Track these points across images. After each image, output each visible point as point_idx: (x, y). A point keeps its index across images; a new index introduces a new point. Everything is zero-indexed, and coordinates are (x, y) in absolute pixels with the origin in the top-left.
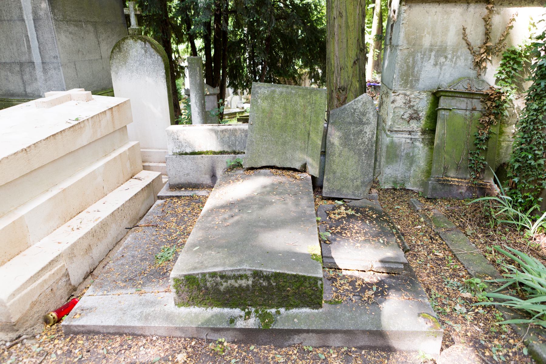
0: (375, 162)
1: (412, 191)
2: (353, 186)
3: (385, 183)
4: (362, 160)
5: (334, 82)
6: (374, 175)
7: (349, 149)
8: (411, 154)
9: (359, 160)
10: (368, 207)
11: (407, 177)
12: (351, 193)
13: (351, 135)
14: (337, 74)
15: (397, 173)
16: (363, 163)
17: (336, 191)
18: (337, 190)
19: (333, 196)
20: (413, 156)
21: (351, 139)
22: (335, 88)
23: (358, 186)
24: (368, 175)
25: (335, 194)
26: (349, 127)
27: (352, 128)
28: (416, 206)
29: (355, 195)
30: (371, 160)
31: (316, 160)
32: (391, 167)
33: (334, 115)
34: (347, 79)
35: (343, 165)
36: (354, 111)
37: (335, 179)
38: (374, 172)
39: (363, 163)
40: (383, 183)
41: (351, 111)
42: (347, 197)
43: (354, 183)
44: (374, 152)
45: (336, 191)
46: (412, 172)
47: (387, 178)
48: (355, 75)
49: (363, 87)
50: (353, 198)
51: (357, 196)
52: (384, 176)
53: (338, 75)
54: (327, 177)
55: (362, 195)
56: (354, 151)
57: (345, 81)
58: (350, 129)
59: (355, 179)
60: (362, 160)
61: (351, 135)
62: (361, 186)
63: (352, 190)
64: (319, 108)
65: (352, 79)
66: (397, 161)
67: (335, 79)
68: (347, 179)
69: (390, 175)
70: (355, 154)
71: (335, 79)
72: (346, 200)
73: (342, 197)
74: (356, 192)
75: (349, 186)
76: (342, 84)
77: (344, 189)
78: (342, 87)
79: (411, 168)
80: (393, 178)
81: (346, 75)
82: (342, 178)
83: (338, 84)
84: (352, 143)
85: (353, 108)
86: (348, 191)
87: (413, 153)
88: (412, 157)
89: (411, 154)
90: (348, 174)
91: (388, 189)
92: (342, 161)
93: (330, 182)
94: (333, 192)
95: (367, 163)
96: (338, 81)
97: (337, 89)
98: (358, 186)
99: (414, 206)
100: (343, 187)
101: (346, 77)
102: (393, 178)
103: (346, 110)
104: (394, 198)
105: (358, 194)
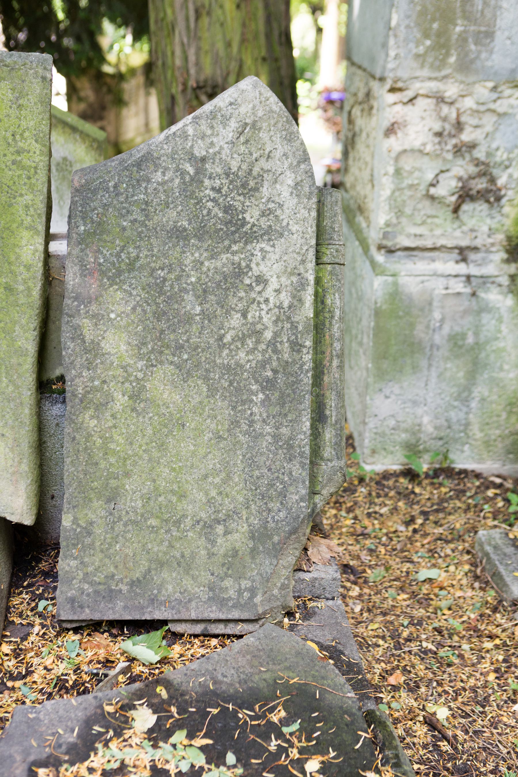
0: (314, 427)
1: (478, 476)
2: (211, 555)
3: (374, 452)
4: (251, 423)
5: (178, 62)
6: (313, 493)
7: (179, 367)
8: (470, 340)
9: (236, 423)
10: (287, 688)
11: (456, 427)
12: (203, 594)
13: (189, 297)
14: (184, 33)
15: (419, 411)
16: (257, 437)
17: (125, 588)
18: (132, 584)
19: (111, 616)
20: (478, 346)
21: (189, 319)
22: (180, 88)
23: (235, 553)
24: (283, 494)
25: (120, 604)
26: (176, 253)
27: (188, 260)
28: (508, 579)
29: (222, 603)
30: (297, 421)
32: (396, 389)
33: (95, 192)
34: (222, 53)
35: (155, 454)
36: (197, 173)
37: (119, 527)
38: (313, 477)
39: (257, 437)
40: (367, 451)
41: (183, 173)
42: (184, 616)
43: (213, 542)
44: (307, 379)
45: (125, 588)
46: (474, 404)
47: (383, 435)
48: (250, 36)
49: (286, 82)
50: (213, 616)
51: (234, 606)
52: (371, 425)
53: (189, 38)
54: (75, 521)
55: (258, 599)
56: (206, 379)
57: (216, 60)
58: (181, 264)
59: (218, 522)
60: (251, 423)
61: (189, 297)
62: (254, 552)
63: (205, 577)
64: (10, 157)
65: (240, 51)
66: (415, 368)
67: (178, 52)
68: (178, 523)
69: (392, 423)
70: (212, 391)
71: (178, 52)
72: (179, 628)
73: (158, 616)
74: (228, 583)
75: (193, 556)
76: (208, 70)
77: (165, 574)
78: (206, 81)
79: (470, 392)
80: (406, 431)
81: (219, 37)
82: (153, 522)
83: (192, 71)
84: (194, 340)
85: (192, 158)
86: (188, 583)
87: (476, 334)
88: (472, 349)
89: (470, 340)
90: (182, 496)
91: (386, 476)
92: (149, 431)
93: (92, 546)
95: (276, 437)
96: (192, 58)
97: (189, 91)
98: (235, 553)
99: (496, 575)
100: (161, 564)
101: (220, 46)
102: (406, 431)
103: (157, 166)
104: (412, 520)
105: (240, 592)
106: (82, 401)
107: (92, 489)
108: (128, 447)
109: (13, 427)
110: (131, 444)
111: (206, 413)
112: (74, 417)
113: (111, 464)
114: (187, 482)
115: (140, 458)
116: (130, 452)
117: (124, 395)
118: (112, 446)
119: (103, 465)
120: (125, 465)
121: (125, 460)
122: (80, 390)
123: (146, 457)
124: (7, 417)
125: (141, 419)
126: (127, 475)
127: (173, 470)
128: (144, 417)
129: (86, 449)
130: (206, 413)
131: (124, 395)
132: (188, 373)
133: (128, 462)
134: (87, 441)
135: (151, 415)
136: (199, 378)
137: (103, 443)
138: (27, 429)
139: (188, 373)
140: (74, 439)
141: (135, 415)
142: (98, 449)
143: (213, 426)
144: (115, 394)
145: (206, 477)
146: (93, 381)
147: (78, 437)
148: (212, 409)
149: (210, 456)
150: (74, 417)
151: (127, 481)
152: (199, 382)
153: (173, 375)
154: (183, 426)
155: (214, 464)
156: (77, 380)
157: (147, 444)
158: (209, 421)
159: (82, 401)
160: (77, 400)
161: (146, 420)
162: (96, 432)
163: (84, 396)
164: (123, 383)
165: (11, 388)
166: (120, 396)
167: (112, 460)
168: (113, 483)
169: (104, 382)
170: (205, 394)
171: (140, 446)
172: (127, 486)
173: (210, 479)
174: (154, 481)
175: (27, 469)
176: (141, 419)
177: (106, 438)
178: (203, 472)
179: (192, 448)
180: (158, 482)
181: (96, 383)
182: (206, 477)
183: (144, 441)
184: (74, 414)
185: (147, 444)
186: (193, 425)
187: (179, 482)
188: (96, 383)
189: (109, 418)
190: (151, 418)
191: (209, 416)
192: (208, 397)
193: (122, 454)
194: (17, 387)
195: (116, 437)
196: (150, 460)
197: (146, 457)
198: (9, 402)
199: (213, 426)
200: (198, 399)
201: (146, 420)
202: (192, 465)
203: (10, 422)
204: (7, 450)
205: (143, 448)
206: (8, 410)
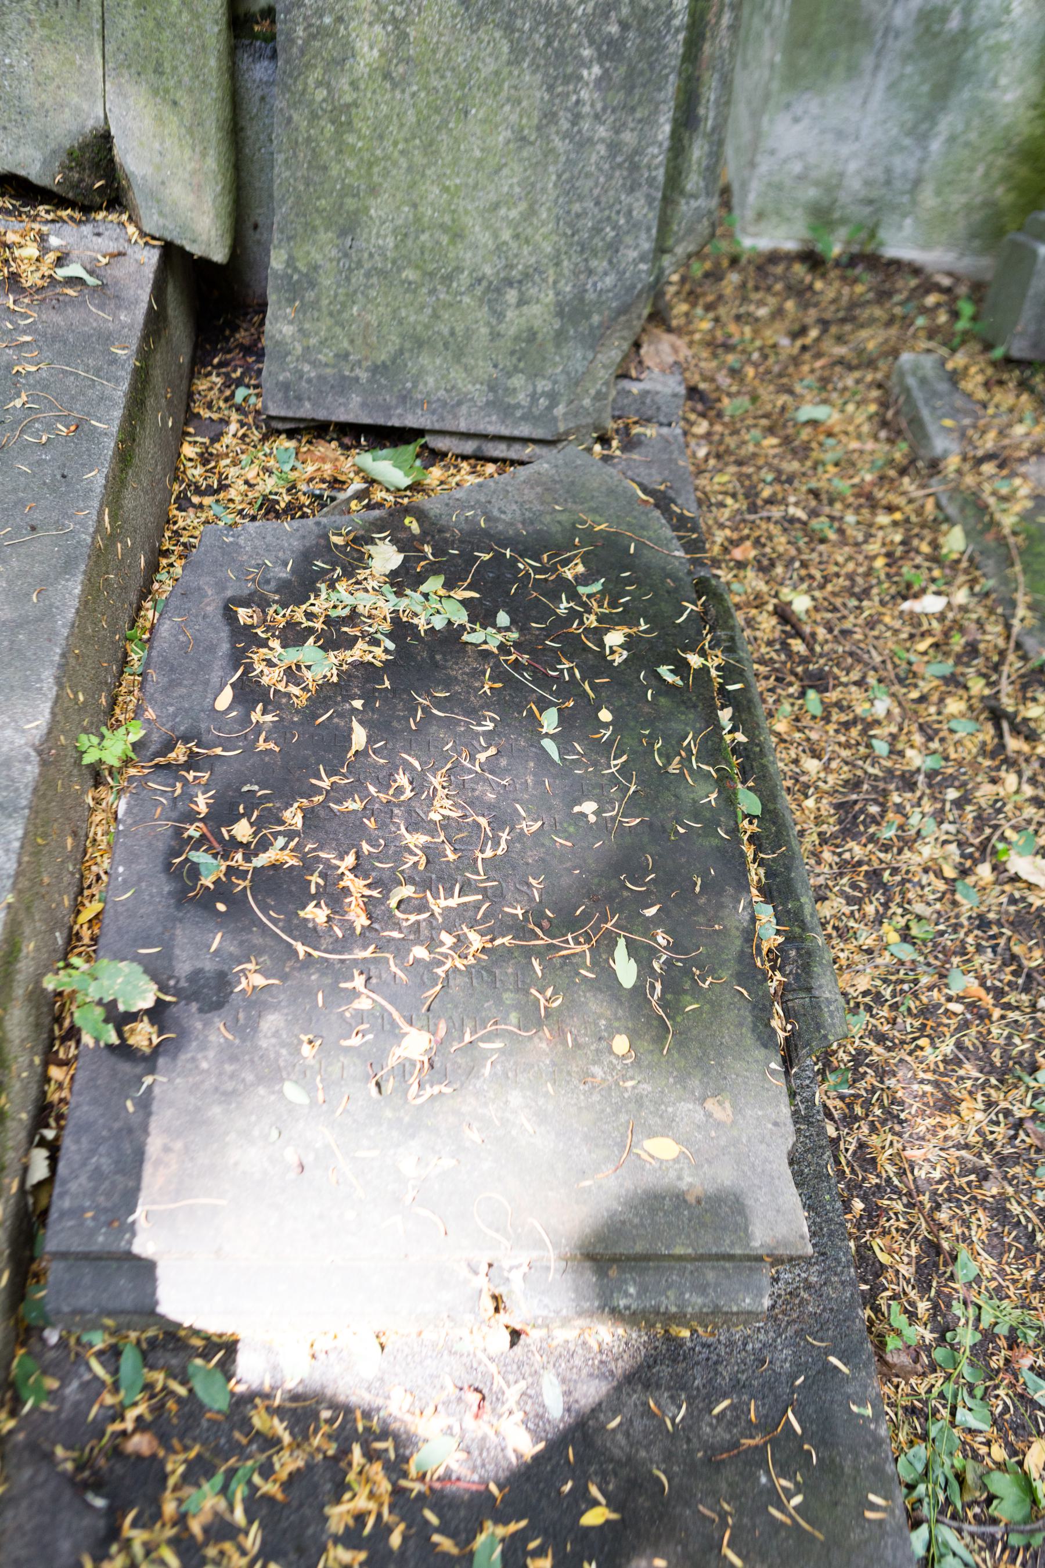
0: (676, 136)
1: (916, 270)
2: (495, 335)
3: (760, 216)
4: (576, 118)
6: (661, 249)
8: (954, 23)
9: (550, 117)
10: (589, 536)
11: (898, 184)
15: (845, 150)
16: (584, 143)
17: (364, 376)
18: (376, 370)
19: (342, 416)
20: (966, 36)
23: (532, 335)
24: (614, 247)
25: (356, 399)
28: (932, 428)
29: (506, 411)
30: (649, 121)
31: (184, 101)
32: (814, 107)
35: (419, 159)
37: (358, 278)
38: (664, 224)
39: (584, 143)
40: (750, 214)
42: (449, 425)
43: (500, 316)
44: (676, 46)
45: (364, 376)
46: (936, 145)
47: (779, 187)
50: (491, 430)
51: (524, 418)
52: (763, 168)
54: (291, 262)
55: (560, 410)
56: (509, 29)
59: (509, 283)
60: (576, 118)
62: (560, 337)
63: (485, 369)
66: (853, 70)
68: (447, 280)
69: (797, 167)
70: (518, 54)
72: (440, 444)
73: (411, 421)
74: (518, 381)
75: (469, 334)
77: (424, 360)
79: (934, 123)
80: (817, 184)
82: (409, 274)
86: (457, 375)
87: (967, 13)
88: (954, 41)
89: (954, 23)
90: (457, 235)
91: (774, 257)
92: (411, 117)
93: (315, 304)
94: (344, 385)
95: (614, 147)
98: (532, 335)
99: (916, 422)
100: (420, 343)
102: (817, 184)
104: (803, 331)
105: (534, 397)
106: (302, 52)
107: (317, 210)
108: (375, 143)
109: (191, 91)
110: (381, 137)
111: (504, 94)
112: (290, 81)
113: (348, 171)
114: (466, 212)
115: (395, 164)
116: (378, 152)
117: (371, 48)
118: (351, 139)
119: (335, 170)
120: (369, 174)
121: (370, 165)
122: (300, 32)
123: (403, 163)
124: (181, 70)
125: (398, 94)
126: (374, 191)
127: (446, 189)
128: (403, 91)
129: (308, 140)
130: (504, 94)
131: (371, 48)
132: (480, 14)
133: (376, 170)
134: (310, 125)
135: (415, 88)
136: (497, 26)
137: (336, 132)
138: (214, 94)
139: (480, 14)
140: (289, 120)
141: (388, 86)
142: (329, 142)
143: (514, 118)
144: (358, 45)
145: (496, 206)
146: (321, 17)
147: (296, 117)
148: (515, 87)
149: (505, 171)
150: (290, 81)
151: (372, 202)
152: (498, 34)
153: (454, 16)
154: (466, 113)
155: (511, 186)
156: (295, 12)
157: (406, 140)
158: (507, 108)
159: (302, 52)
160: (295, 50)
161: (407, 96)
162: (325, 111)
163: (307, 42)
164: (371, 24)
165: (185, 17)
166: (366, 49)
167: (350, 164)
168: (351, 203)
169: (340, 19)
170: (504, 58)
171: (395, 144)
172: (372, 212)
173: (503, 211)
174: (415, 206)
175: (214, 166)
176: (398, 94)
177: (342, 124)
178: (493, 197)
179: (478, 153)
180: (421, 209)
181: (327, 20)
182: (496, 206)
183: (402, 135)
184: (290, 76)
185: (406, 140)
186: (480, 115)
187: (454, 211)
188: (327, 20)
189: (346, 87)
190: (413, 95)
191: (508, 100)
192: (509, 63)
193: (366, 155)
194: (196, 16)
195: (358, 124)
196: (410, 169)
197: (403, 163)
198: (183, 42)
199: (514, 118)
200: (492, 67)
201: (407, 96)
202: (476, 184)
203: (186, 79)
204: (183, 131)
205: (400, 147)
206: (182, 57)
